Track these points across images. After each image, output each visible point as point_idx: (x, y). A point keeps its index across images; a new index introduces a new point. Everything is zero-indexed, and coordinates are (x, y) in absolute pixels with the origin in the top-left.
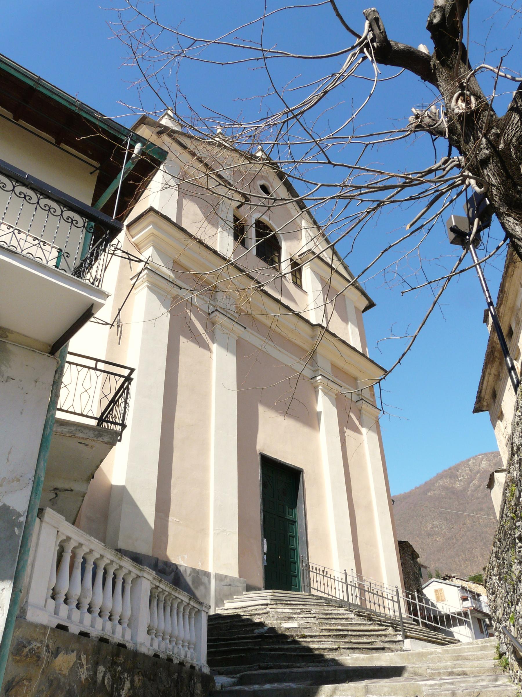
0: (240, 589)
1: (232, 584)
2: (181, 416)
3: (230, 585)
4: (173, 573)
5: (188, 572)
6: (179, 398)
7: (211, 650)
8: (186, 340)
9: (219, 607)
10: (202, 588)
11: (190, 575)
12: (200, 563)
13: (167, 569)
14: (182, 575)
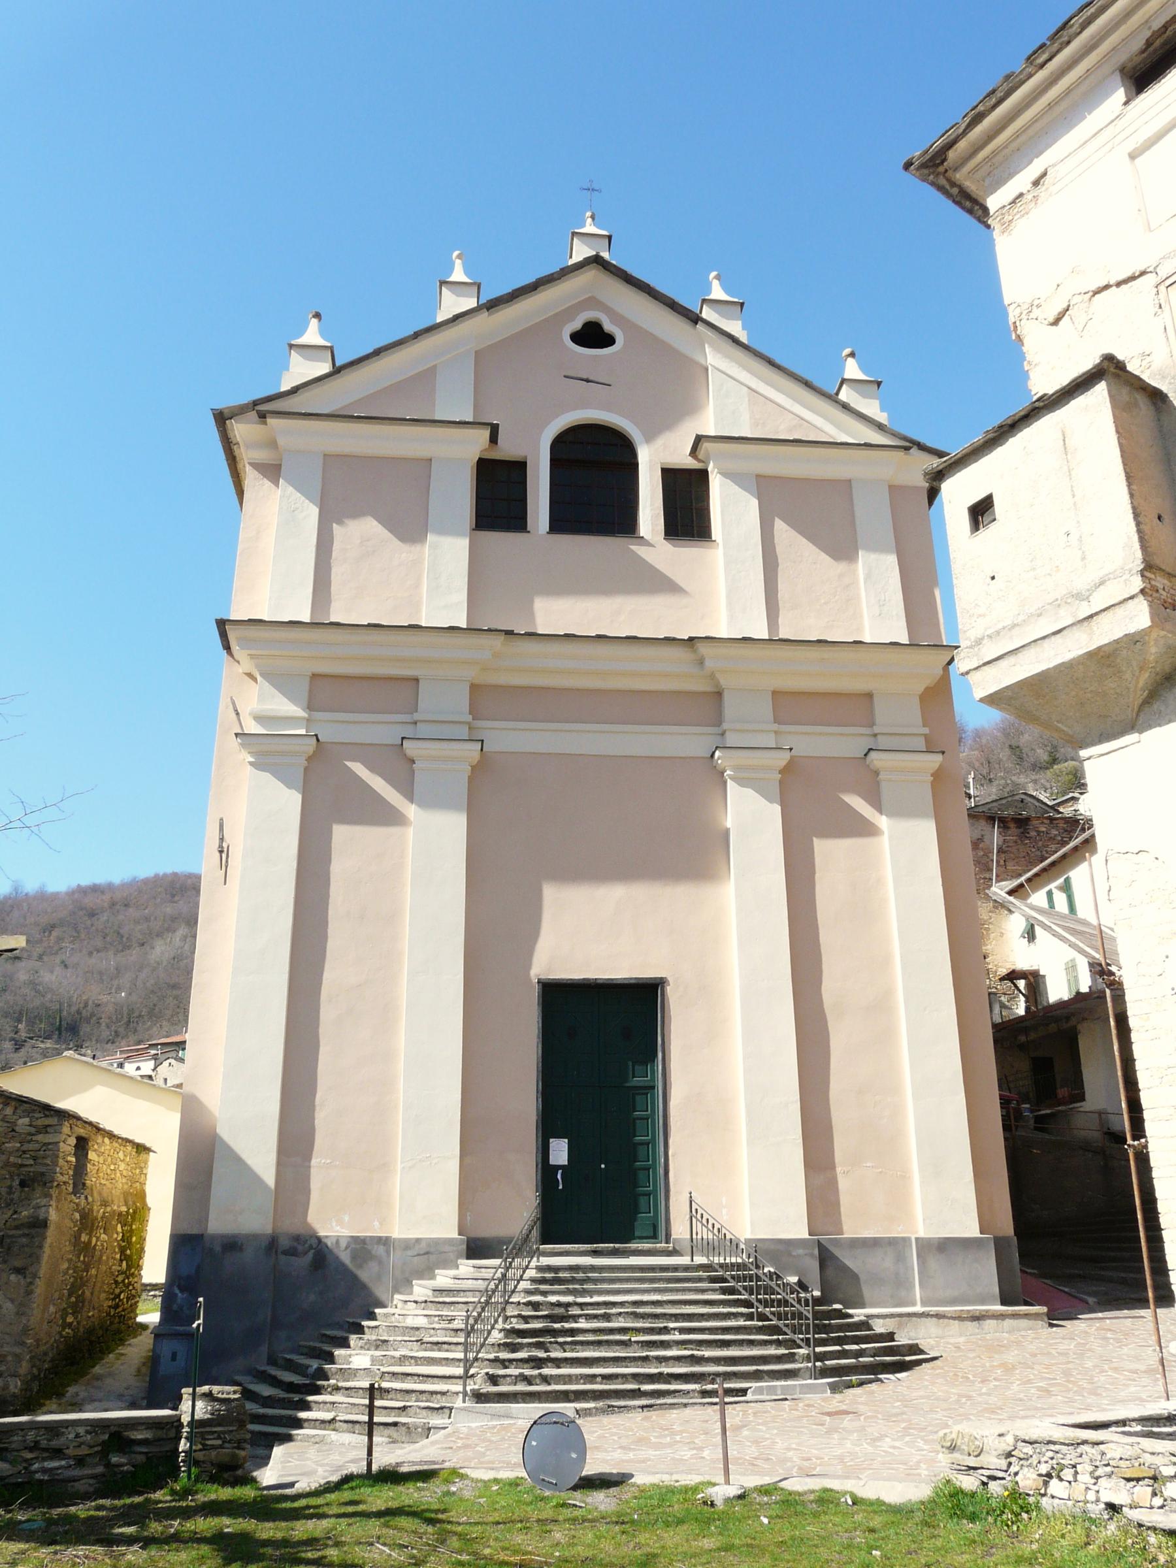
0: (452, 1256)
1: (432, 1250)
2: (336, 975)
3: (427, 1253)
4: (311, 1254)
5: (343, 1244)
6: (331, 945)
7: (1151, 1300)
8: (1106, 393)
9: (400, 1293)
10: (373, 1266)
11: (347, 1248)
12: (376, 1223)
13: (300, 1248)
14: (331, 1251)
